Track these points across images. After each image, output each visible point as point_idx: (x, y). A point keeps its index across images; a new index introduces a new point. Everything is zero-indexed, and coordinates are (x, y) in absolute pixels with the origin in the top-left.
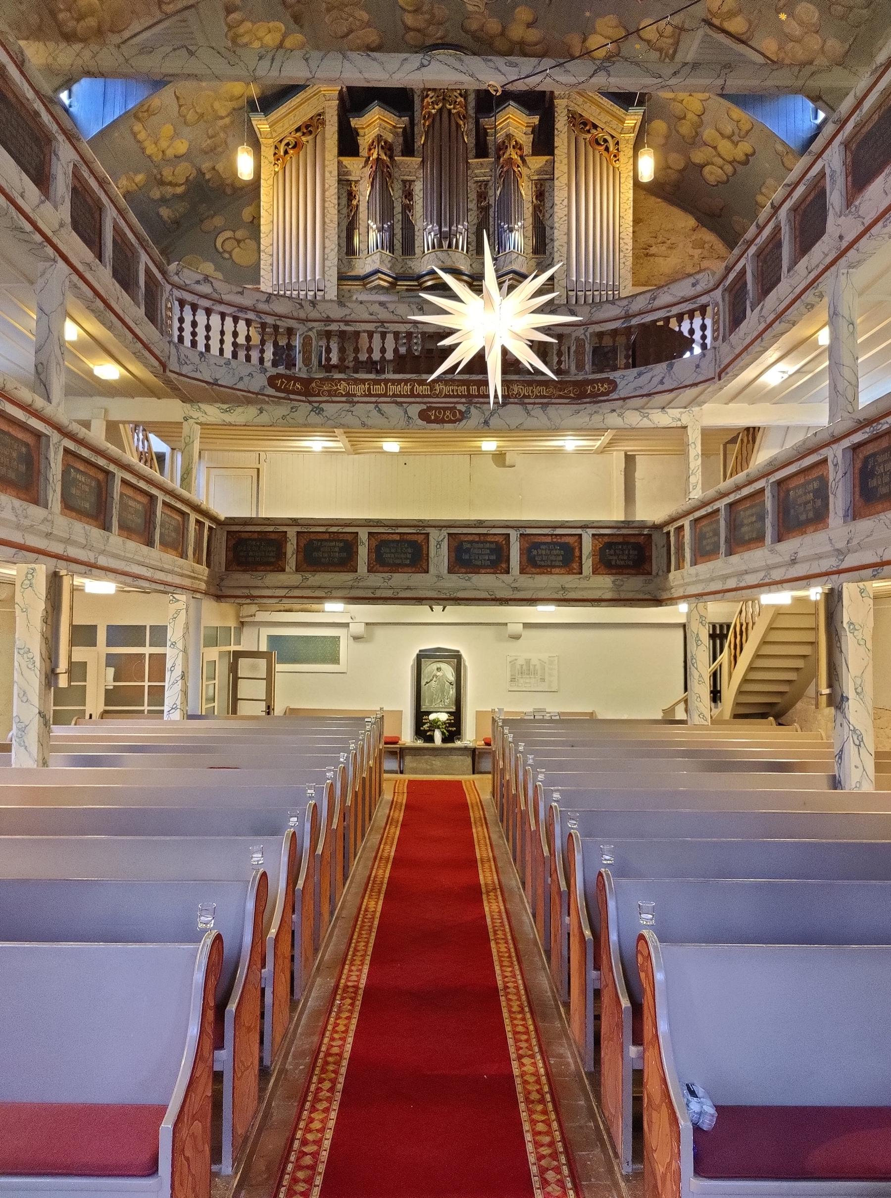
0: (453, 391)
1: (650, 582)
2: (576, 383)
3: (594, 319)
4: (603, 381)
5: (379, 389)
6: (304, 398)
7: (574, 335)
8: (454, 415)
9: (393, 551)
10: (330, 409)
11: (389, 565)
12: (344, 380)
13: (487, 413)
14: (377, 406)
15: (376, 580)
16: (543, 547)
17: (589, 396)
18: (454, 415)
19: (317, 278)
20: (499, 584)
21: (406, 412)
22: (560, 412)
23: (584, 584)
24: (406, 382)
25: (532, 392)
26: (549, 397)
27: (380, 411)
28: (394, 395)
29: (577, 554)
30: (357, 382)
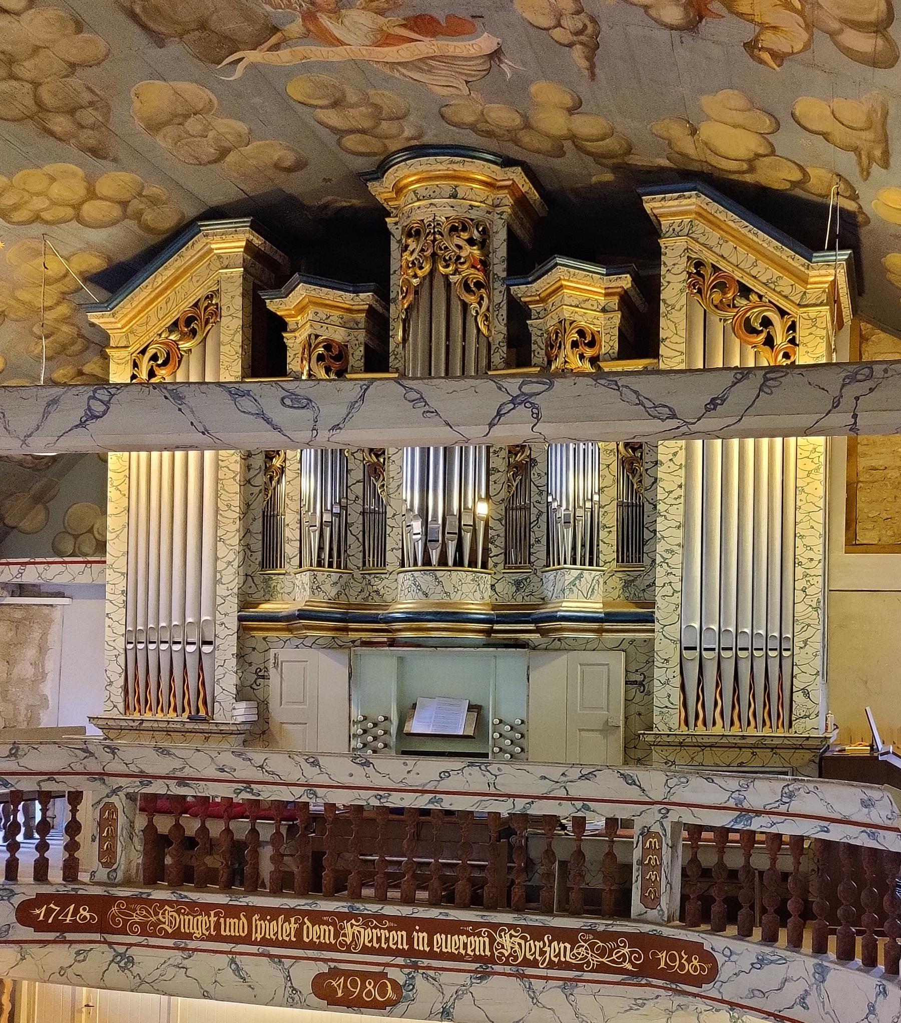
0: (379, 940)
2: (635, 940)
3: (674, 799)
5: (235, 926)
6: (97, 936)
8: (383, 991)
10: (149, 959)
12: (169, 903)
13: (449, 991)
14: (233, 961)
17: (662, 975)
18: (383, 991)
21: (288, 978)
25: (542, 953)
27: (238, 970)
28: (265, 942)
30: (196, 908)
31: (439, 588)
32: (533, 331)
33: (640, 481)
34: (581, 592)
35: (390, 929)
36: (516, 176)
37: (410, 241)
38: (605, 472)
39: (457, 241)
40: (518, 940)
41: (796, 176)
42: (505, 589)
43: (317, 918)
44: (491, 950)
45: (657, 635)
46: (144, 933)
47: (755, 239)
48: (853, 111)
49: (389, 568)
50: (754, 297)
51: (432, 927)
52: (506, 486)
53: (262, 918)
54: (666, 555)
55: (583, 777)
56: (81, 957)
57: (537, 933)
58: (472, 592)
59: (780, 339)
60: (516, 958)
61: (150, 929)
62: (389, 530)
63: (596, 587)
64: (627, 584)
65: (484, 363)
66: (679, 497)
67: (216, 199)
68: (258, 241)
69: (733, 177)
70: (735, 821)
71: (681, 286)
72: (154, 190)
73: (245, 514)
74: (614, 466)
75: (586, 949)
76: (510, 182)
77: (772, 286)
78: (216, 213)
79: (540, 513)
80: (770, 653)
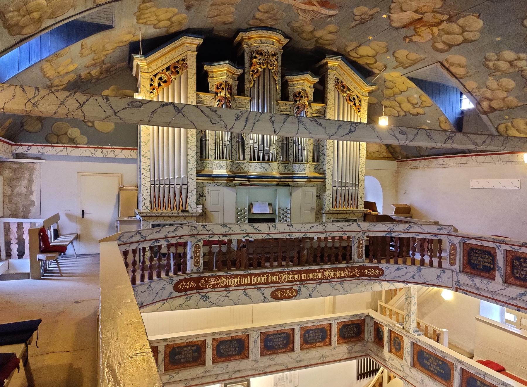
0: (292, 278)
1: (364, 346)
4: (375, 268)
5: (246, 281)
6: (195, 291)
8: (292, 293)
9: (227, 347)
10: (214, 296)
12: (223, 276)
13: (311, 290)
14: (244, 292)
17: (367, 276)
18: (292, 293)
19: (182, 176)
22: (350, 285)
23: (334, 352)
24: (264, 274)
25: (336, 275)
26: (345, 277)
27: (246, 295)
29: (329, 333)
30: (232, 277)
32: (290, 91)
35: (295, 274)
42: (282, 168)
43: (273, 274)
46: (214, 287)
49: (246, 161)
51: (307, 272)
53: (255, 277)
56: (188, 299)
57: (335, 269)
62: (245, 148)
64: (315, 168)
70: (387, 234)
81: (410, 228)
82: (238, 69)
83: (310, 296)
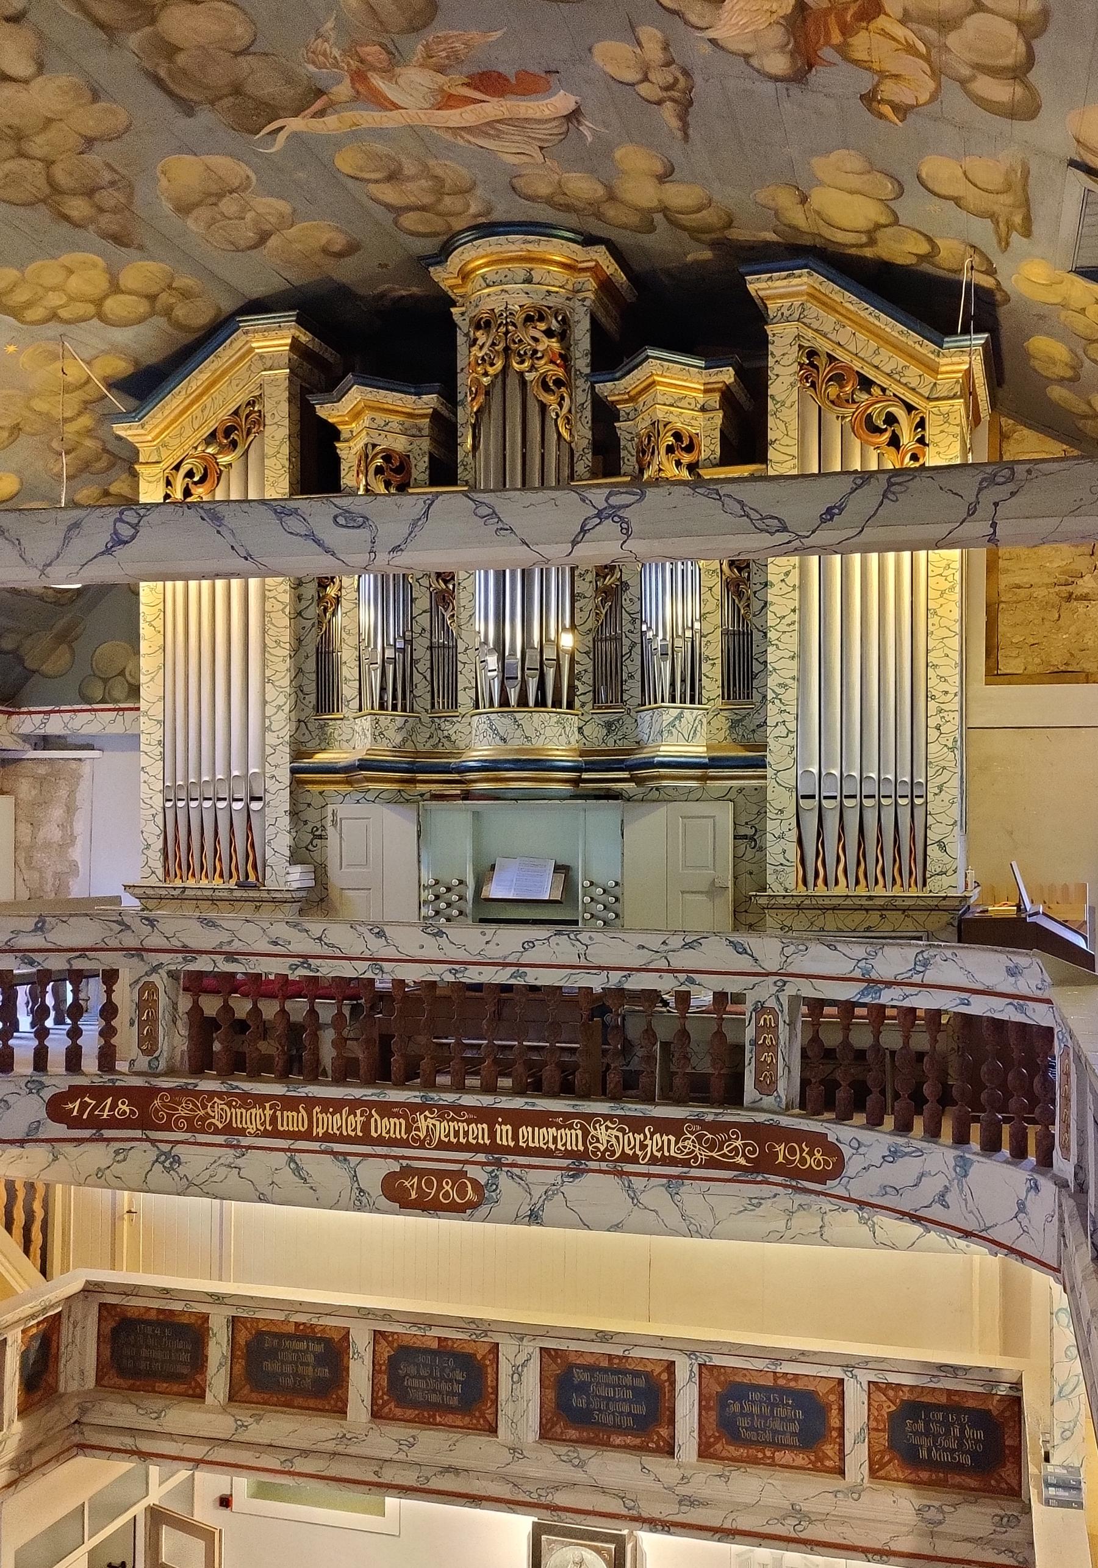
0: (457, 1134)
2: (749, 1131)
3: (790, 970)
6: (138, 1133)
7: (751, 998)
8: (462, 1192)
10: (196, 1159)
11: (414, 1405)
12: (220, 1095)
13: (538, 1192)
14: (292, 1160)
15: (384, 1441)
16: (756, 1396)
17: (779, 1170)
18: (462, 1192)
20: (646, 1482)
23: (847, 1506)
25: (643, 1147)
26: (685, 1163)
27: (297, 1170)
28: (328, 1137)
29: (835, 1422)
31: (519, 732)
32: (623, 435)
33: (748, 606)
34: (682, 734)
36: (600, 256)
37: (479, 334)
38: (707, 596)
39: (533, 332)
40: (615, 1132)
41: (924, 248)
42: (595, 732)
43: (387, 1109)
44: (584, 1144)
45: (770, 783)
46: (191, 1129)
47: (877, 322)
48: (989, 170)
50: (876, 391)
52: (593, 614)
53: (324, 1111)
54: (778, 690)
55: (688, 946)
56: (120, 1157)
57: (636, 1125)
58: (557, 736)
59: (907, 438)
60: (613, 1153)
61: (197, 1124)
62: (460, 666)
63: (699, 728)
64: (734, 724)
65: (566, 472)
66: (793, 623)
67: (257, 290)
68: (305, 338)
69: (853, 251)
70: (862, 993)
71: (792, 379)
72: (184, 281)
73: (296, 651)
74: (717, 589)
75: (693, 1141)
76: (593, 264)
77: (897, 377)
78: (256, 307)
79: (634, 644)
80: (901, 801)
81: (926, 964)
82: (418, 394)
83: (534, 1217)
